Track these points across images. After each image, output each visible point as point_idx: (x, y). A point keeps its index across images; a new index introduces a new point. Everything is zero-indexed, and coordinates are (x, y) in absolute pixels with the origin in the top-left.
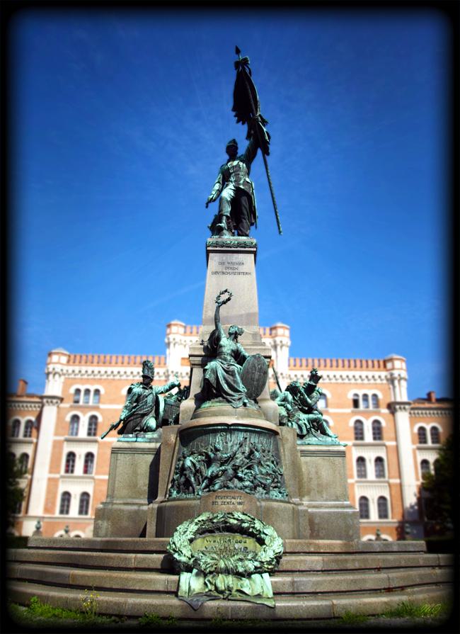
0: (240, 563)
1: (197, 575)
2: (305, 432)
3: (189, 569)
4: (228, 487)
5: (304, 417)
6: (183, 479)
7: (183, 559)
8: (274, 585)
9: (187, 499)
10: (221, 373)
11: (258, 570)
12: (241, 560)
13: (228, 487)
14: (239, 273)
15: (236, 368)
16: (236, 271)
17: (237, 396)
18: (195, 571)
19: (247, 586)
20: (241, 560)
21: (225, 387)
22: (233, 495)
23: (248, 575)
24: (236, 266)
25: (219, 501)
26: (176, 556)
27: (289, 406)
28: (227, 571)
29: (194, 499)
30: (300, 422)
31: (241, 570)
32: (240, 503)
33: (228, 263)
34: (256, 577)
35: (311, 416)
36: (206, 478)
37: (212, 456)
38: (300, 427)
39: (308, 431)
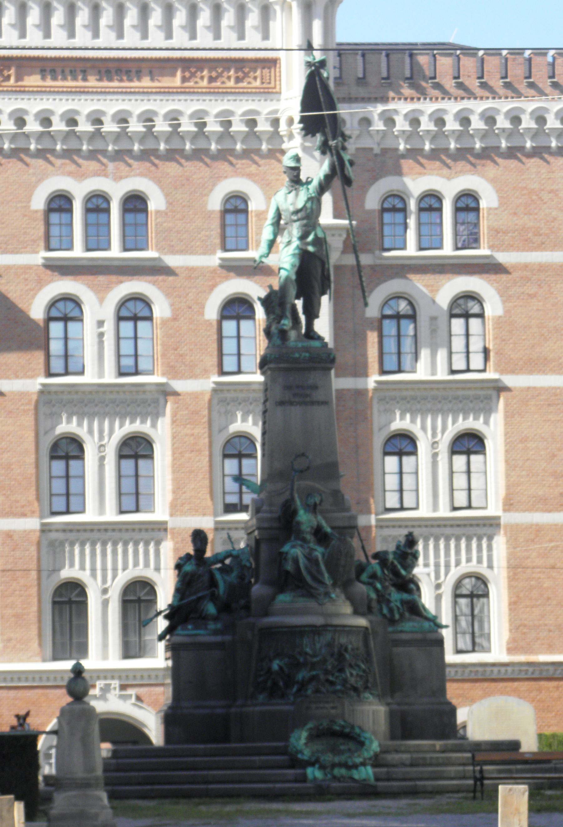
2: (397, 616)
5: (396, 596)
6: (269, 683)
8: (375, 774)
10: (302, 561)
14: (313, 403)
15: (319, 552)
16: (308, 399)
17: (322, 590)
19: (356, 775)
21: (308, 578)
24: (308, 392)
27: (379, 586)
30: (392, 605)
33: (298, 387)
34: (362, 769)
35: (405, 596)
36: (297, 682)
37: (301, 660)
38: (391, 610)
39: (402, 615)
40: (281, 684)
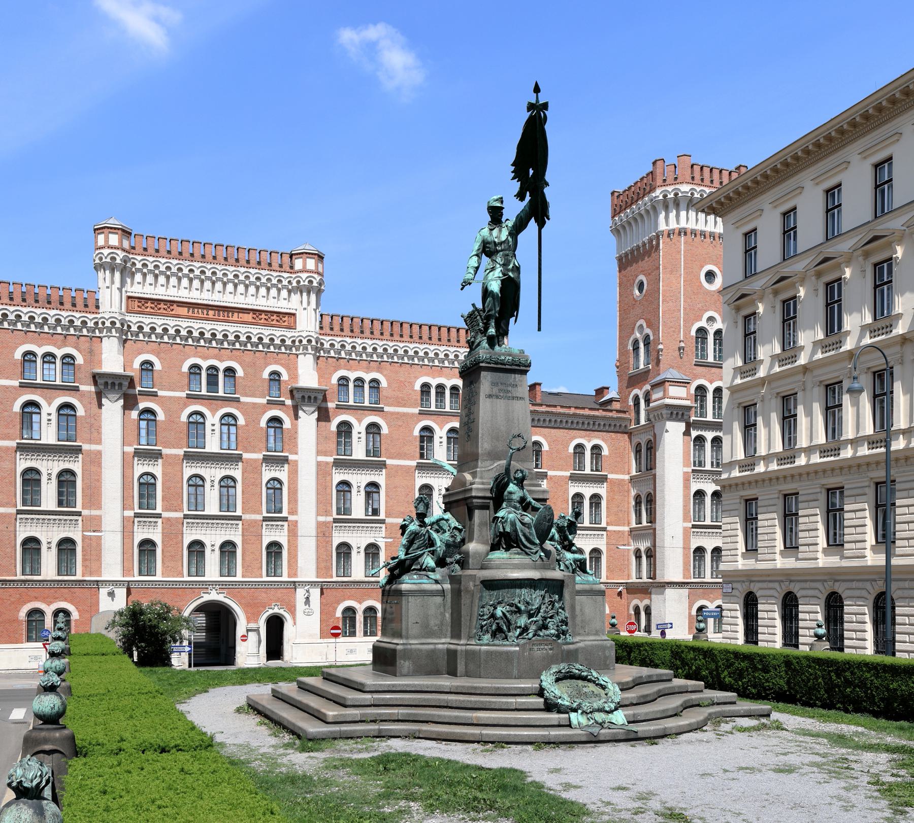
0: (606, 705)
1: (582, 713)
3: (575, 710)
4: (539, 636)
7: (567, 703)
9: (505, 645)
11: (616, 709)
13: (539, 636)
18: (580, 711)
23: (611, 712)
25: (535, 648)
26: (559, 701)
29: (511, 646)
31: (608, 709)
32: (551, 649)
40: (505, 628)
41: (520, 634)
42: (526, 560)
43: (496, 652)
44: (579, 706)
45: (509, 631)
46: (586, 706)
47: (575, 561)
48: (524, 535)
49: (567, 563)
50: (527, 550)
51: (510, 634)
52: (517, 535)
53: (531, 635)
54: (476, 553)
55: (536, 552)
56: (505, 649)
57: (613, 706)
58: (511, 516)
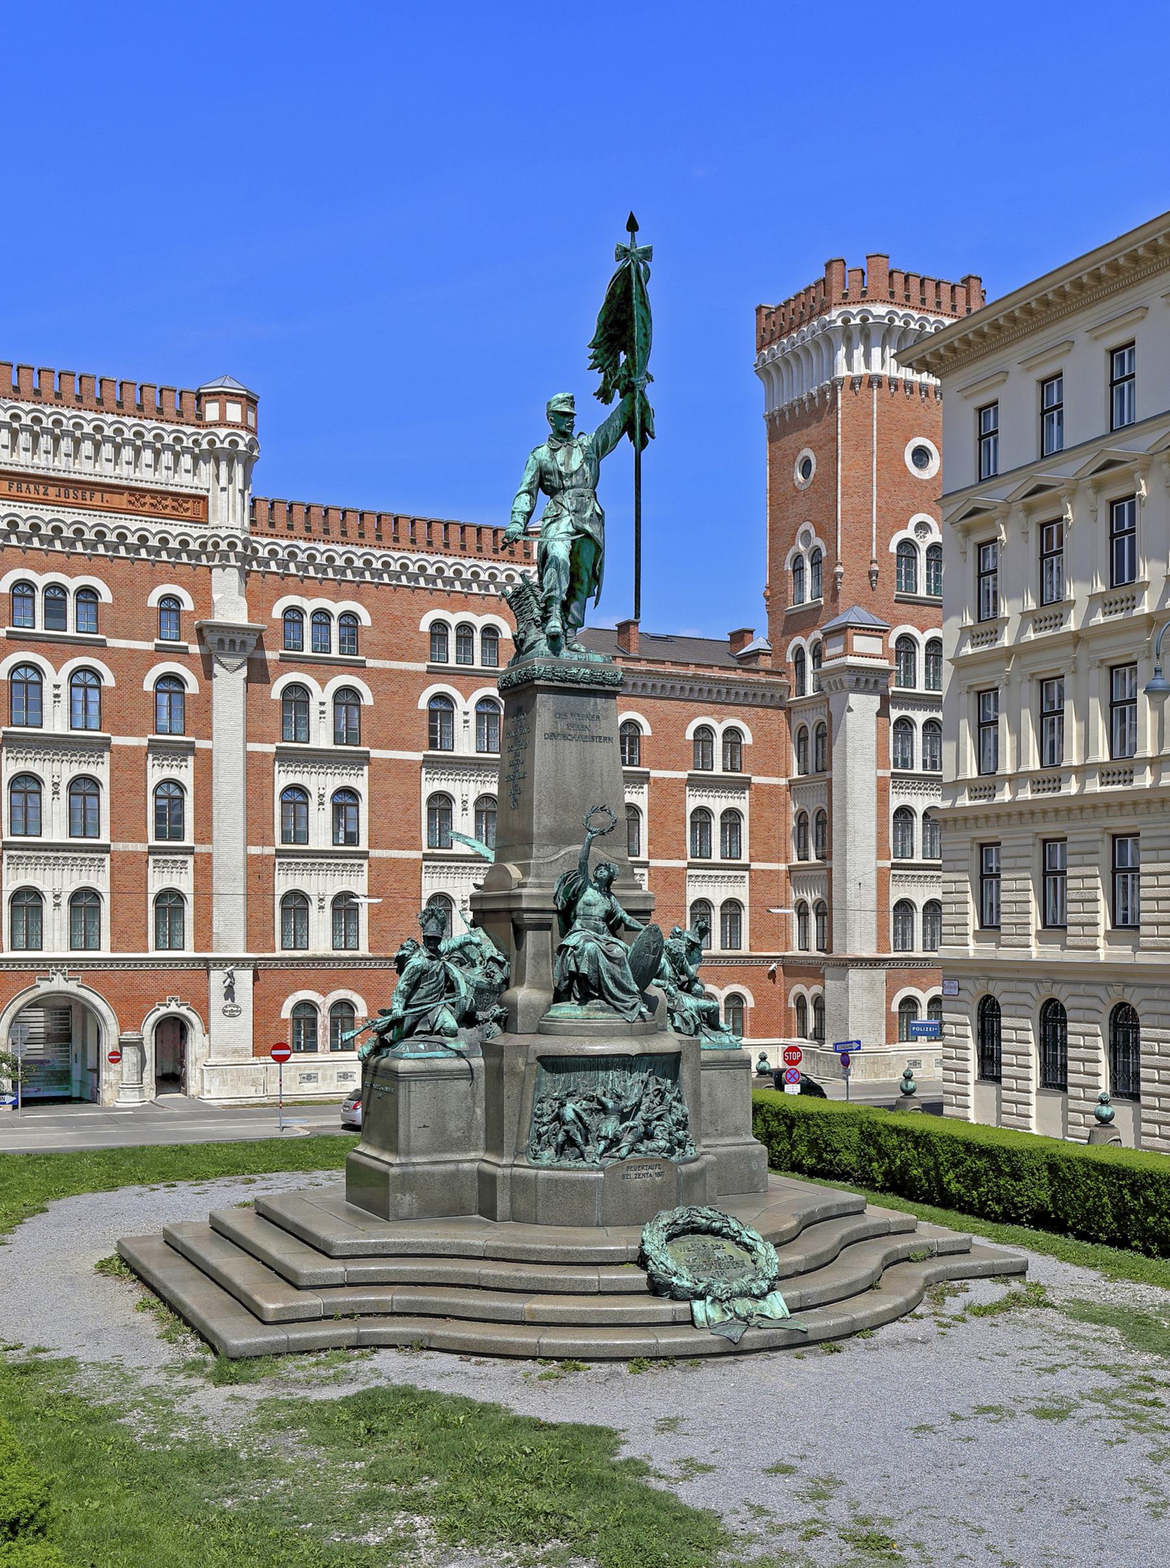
0: (754, 1285)
1: (712, 1302)
3: (701, 1297)
4: (639, 1151)
7: (688, 1284)
9: (579, 1169)
12: (753, 1280)
13: (639, 1151)
18: (709, 1299)
20: (753, 1280)
22: (649, 1164)
23: (763, 1296)
25: (632, 1173)
26: (674, 1280)
28: (743, 1294)
29: (591, 1170)
31: (756, 1292)
32: (658, 1175)
40: (579, 1139)
41: (606, 1150)
42: (616, 1020)
43: (565, 1181)
44: (708, 1289)
45: (587, 1142)
46: (719, 1288)
47: (700, 1011)
48: (613, 978)
49: (686, 1014)
50: (618, 1004)
51: (589, 1148)
52: (600, 978)
53: (624, 1151)
54: (530, 1006)
55: (634, 1006)
56: (580, 1175)
57: (765, 1285)
58: (590, 946)
